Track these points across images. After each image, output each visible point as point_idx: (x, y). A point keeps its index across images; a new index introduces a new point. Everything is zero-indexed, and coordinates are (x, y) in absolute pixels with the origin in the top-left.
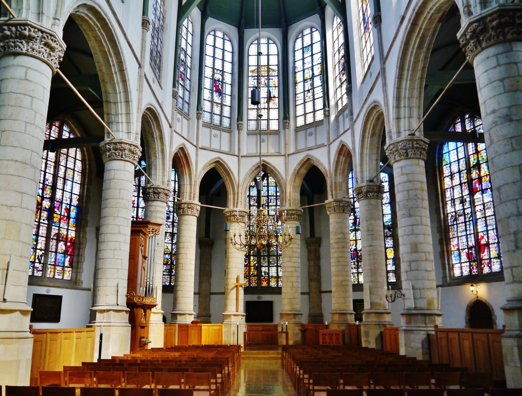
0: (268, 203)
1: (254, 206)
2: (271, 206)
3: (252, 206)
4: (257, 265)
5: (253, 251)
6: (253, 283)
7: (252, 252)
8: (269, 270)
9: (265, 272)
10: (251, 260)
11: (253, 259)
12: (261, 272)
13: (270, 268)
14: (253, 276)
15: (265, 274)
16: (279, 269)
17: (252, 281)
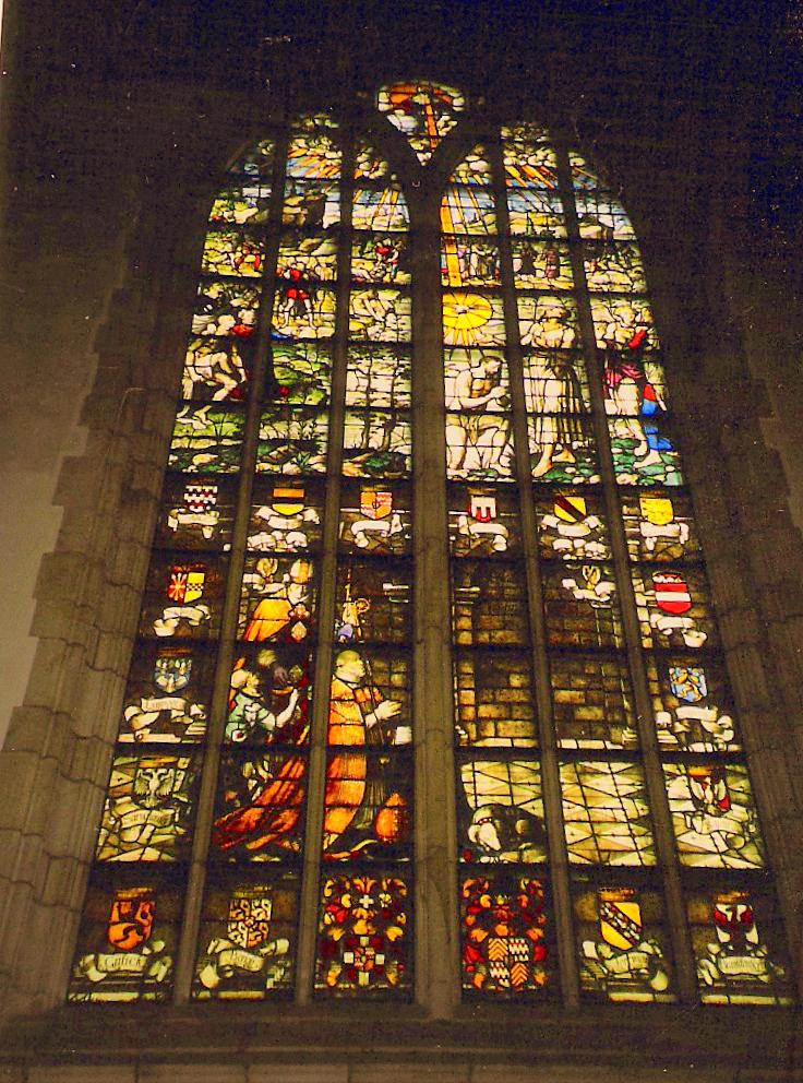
0: (506, 274)
1: (379, 285)
2: (535, 293)
3: (363, 285)
4: (402, 735)
5: (364, 605)
6: (351, 943)
7: (351, 613)
8: (550, 792)
9: (504, 815)
10: (339, 688)
11: (363, 683)
12: (464, 814)
13: (566, 772)
14: (358, 865)
15: (508, 839)
16: (677, 788)
17: (347, 920)
